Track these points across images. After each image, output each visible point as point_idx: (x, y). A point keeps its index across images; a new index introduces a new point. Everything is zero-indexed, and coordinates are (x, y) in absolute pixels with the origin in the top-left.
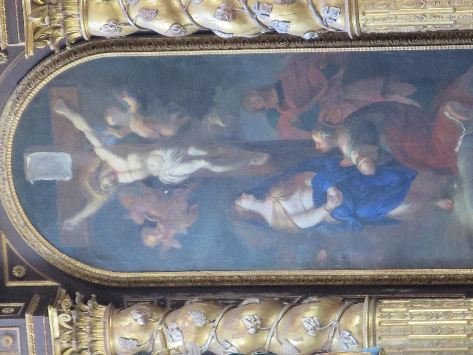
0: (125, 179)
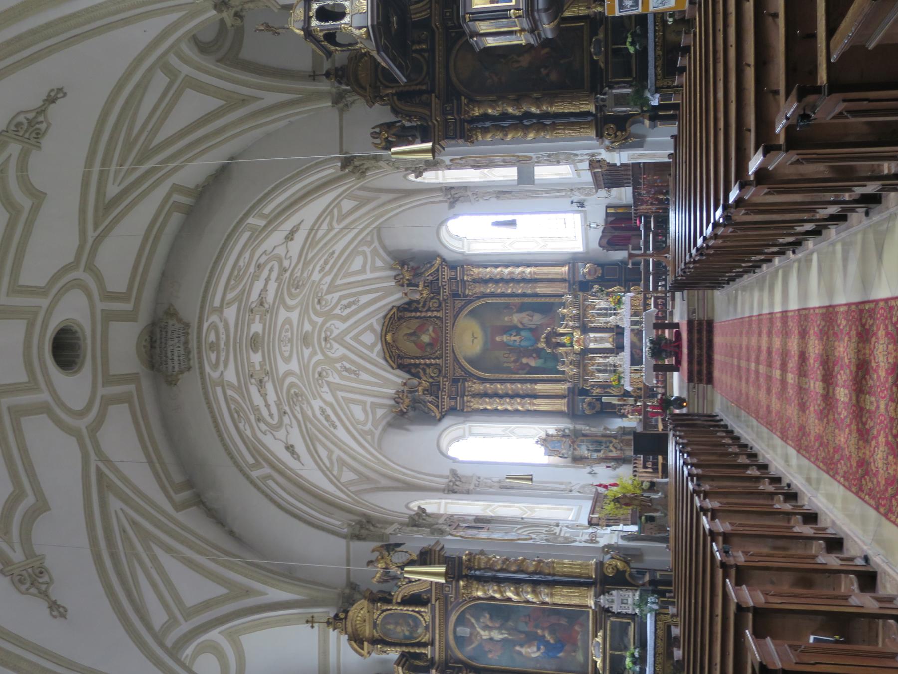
0: (484, 637)
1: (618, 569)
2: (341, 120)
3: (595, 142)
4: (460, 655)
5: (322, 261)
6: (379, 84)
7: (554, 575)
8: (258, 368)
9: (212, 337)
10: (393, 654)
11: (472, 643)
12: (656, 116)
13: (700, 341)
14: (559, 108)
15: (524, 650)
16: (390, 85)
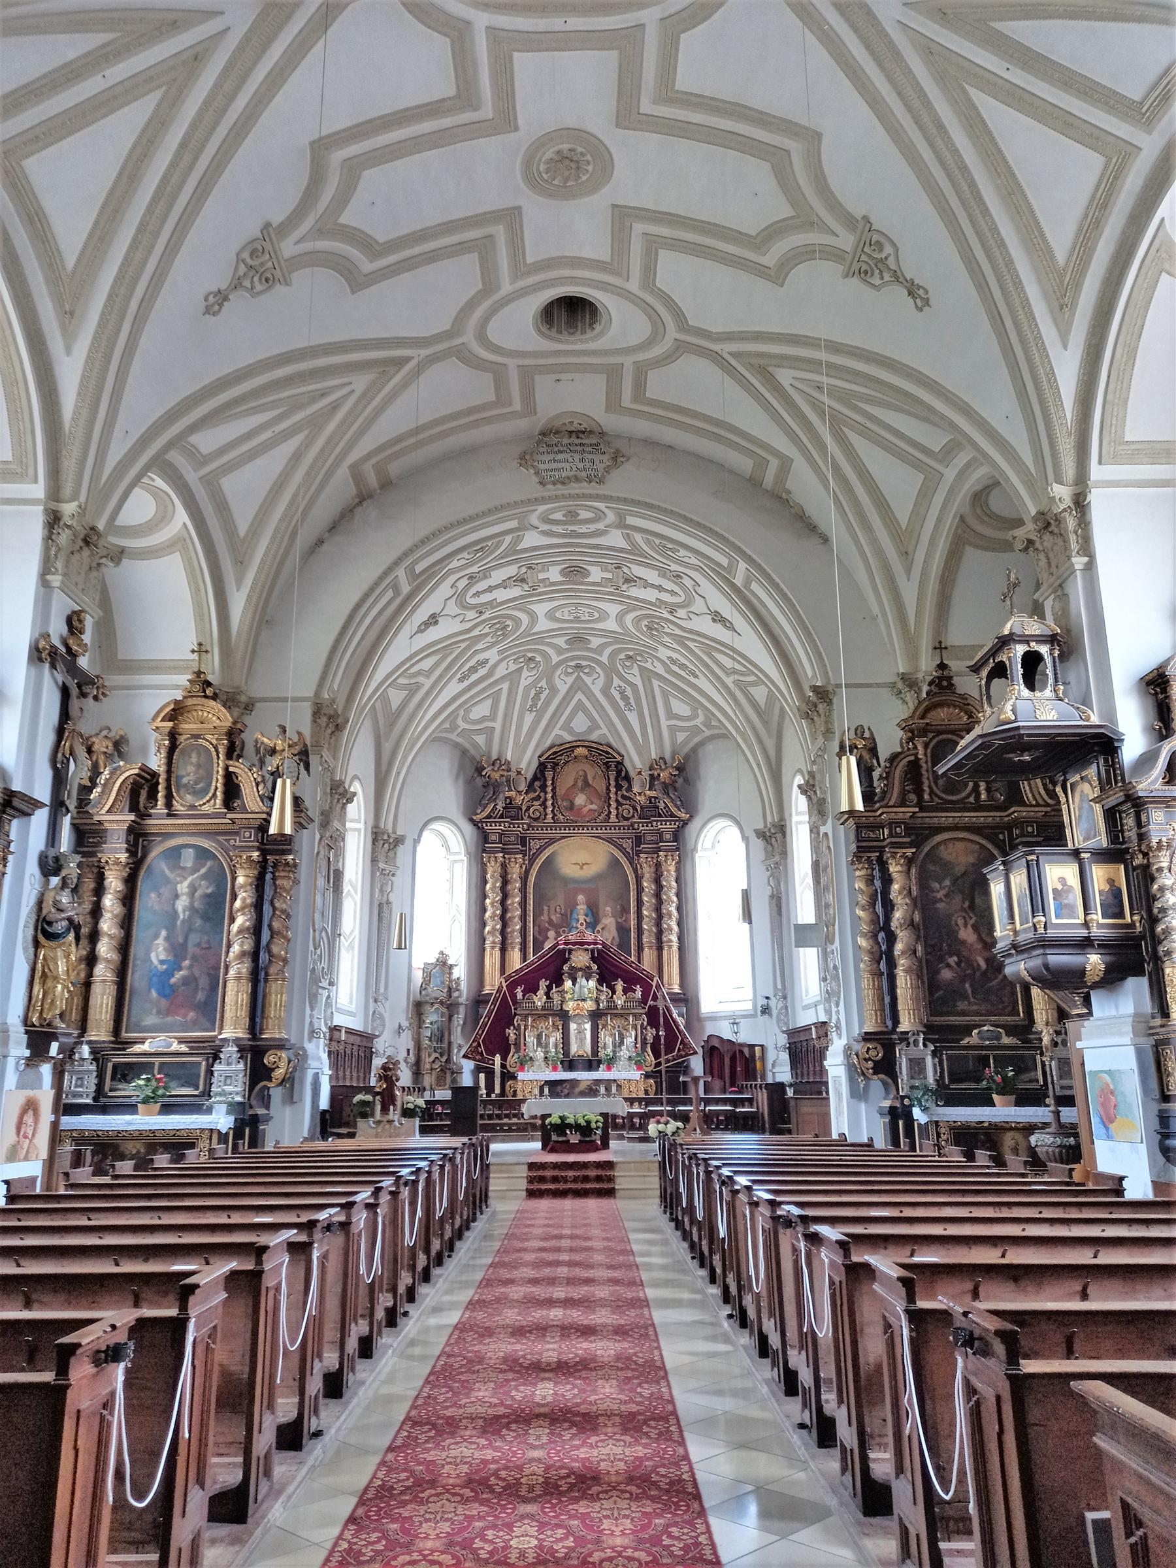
1: (273, 1070)
2: (878, 685)
3: (856, 1032)
4: (153, 854)
5: (684, 661)
6: (931, 735)
7: (266, 981)
8: (541, 576)
9: (584, 514)
10: (156, 762)
11: (172, 869)
12: (898, 1116)
13: (586, 1179)
14: (904, 983)
15: (160, 941)
16: (929, 751)
